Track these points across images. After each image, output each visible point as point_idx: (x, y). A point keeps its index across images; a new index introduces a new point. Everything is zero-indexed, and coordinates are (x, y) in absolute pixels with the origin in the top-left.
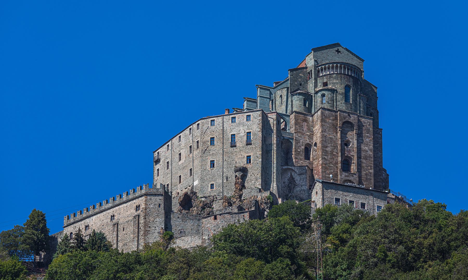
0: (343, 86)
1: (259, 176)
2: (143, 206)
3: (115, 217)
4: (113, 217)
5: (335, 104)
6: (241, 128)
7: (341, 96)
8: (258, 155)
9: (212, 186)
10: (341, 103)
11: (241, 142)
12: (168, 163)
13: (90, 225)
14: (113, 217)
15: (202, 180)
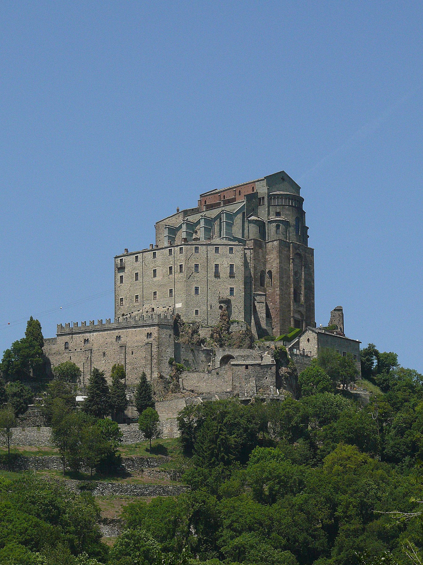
0: (294, 218)
1: (242, 309)
2: (155, 335)
3: (122, 339)
4: (118, 338)
5: (288, 235)
6: (224, 259)
7: (293, 228)
8: (241, 288)
9: (197, 312)
10: (293, 235)
11: (224, 272)
12: (137, 274)
13: (91, 340)
14: (118, 338)
15: (187, 304)
